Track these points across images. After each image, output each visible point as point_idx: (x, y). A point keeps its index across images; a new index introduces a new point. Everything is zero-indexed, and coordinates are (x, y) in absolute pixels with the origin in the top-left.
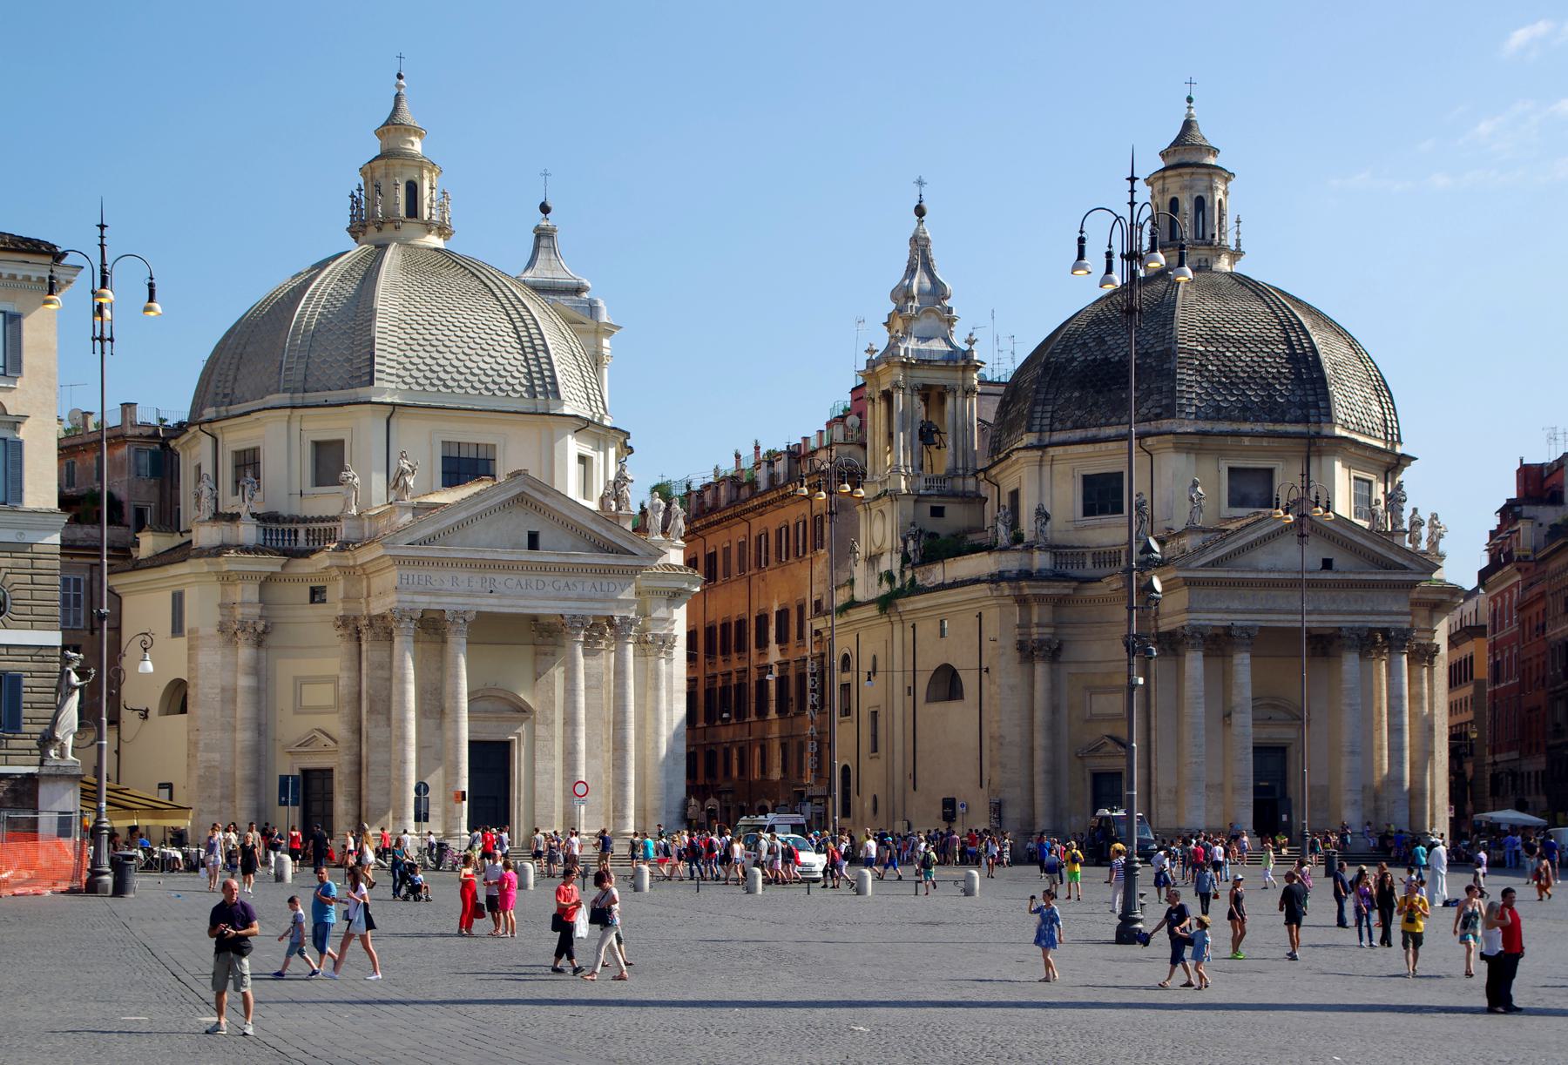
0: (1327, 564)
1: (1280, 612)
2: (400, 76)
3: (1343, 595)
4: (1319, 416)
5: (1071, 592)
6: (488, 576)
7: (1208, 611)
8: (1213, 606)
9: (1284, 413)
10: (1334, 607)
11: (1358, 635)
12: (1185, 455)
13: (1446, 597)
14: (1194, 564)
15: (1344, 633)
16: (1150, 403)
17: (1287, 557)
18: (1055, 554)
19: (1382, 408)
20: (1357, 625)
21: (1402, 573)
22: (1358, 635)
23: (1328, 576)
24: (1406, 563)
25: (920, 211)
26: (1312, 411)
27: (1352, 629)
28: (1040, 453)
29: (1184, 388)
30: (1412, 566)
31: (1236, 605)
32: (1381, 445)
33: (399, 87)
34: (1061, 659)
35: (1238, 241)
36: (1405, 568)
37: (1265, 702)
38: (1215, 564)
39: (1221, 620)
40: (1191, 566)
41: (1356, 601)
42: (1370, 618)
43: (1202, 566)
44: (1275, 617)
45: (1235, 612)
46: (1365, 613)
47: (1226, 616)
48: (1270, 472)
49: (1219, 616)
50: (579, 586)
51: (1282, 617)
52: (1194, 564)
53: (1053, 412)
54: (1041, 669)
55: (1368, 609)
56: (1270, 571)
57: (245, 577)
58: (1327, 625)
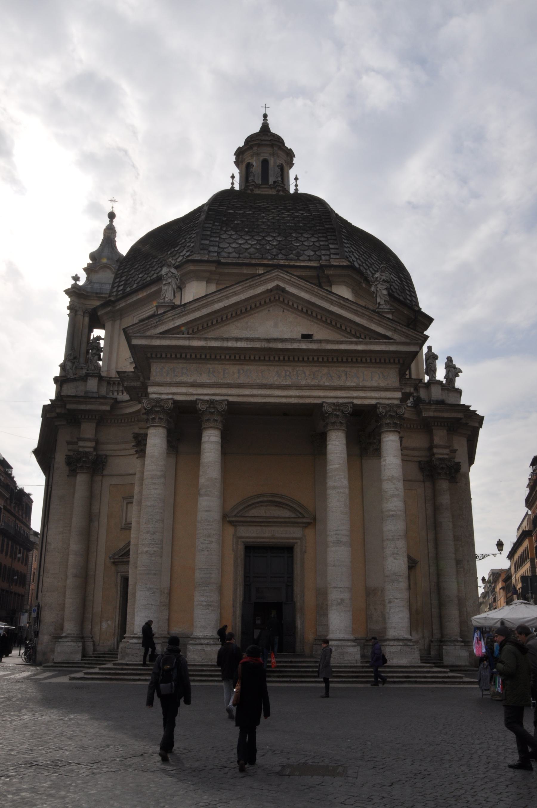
1: (251, 386)
3: (325, 370)
4: (329, 255)
5: (108, 408)
7: (171, 384)
8: (178, 380)
9: (298, 255)
10: (314, 382)
11: (342, 412)
13: (459, 415)
15: (326, 408)
16: (184, 252)
18: (109, 383)
19: (401, 281)
20: (340, 401)
21: (385, 343)
22: (342, 412)
24: (389, 334)
25: (112, 216)
26: (323, 252)
27: (334, 404)
28: (109, 309)
29: (209, 233)
30: (396, 337)
31: (204, 379)
34: (105, 472)
37: (265, 499)
39: (186, 394)
40: (148, 333)
41: (339, 377)
42: (355, 394)
43: (160, 333)
44: (247, 392)
45: (202, 385)
46: (349, 388)
47: (191, 390)
49: (183, 390)
51: (256, 392)
53: (126, 280)
54: (81, 479)
55: (353, 384)
56: (237, 339)
58: (307, 401)
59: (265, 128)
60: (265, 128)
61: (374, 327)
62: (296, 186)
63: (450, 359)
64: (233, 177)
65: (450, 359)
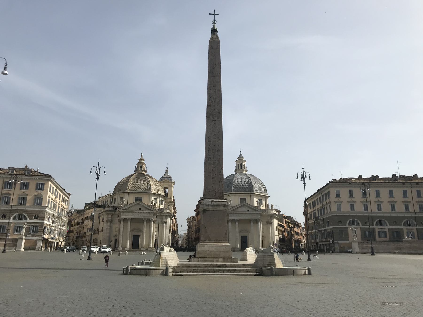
0: (248, 211)
2: (142, 154)
6: (133, 214)
12: (233, 196)
13: (272, 215)
14: (229, 211)
17: (245, 209)
23: (248, 212)
32: (264, 195)
33: (142, 155)
35: (247, 169)
36: (258, 211)
38: (233, 210)
48: (246, 198)
50: (146, 215)
52: (229, 211)
57: (110, 214)
59: (241, 155)
60: (241, 155)
61: (257, 210)
62: (247, 168)
63: (272, 204)
64: (235, 166)
65: (272, 204)
